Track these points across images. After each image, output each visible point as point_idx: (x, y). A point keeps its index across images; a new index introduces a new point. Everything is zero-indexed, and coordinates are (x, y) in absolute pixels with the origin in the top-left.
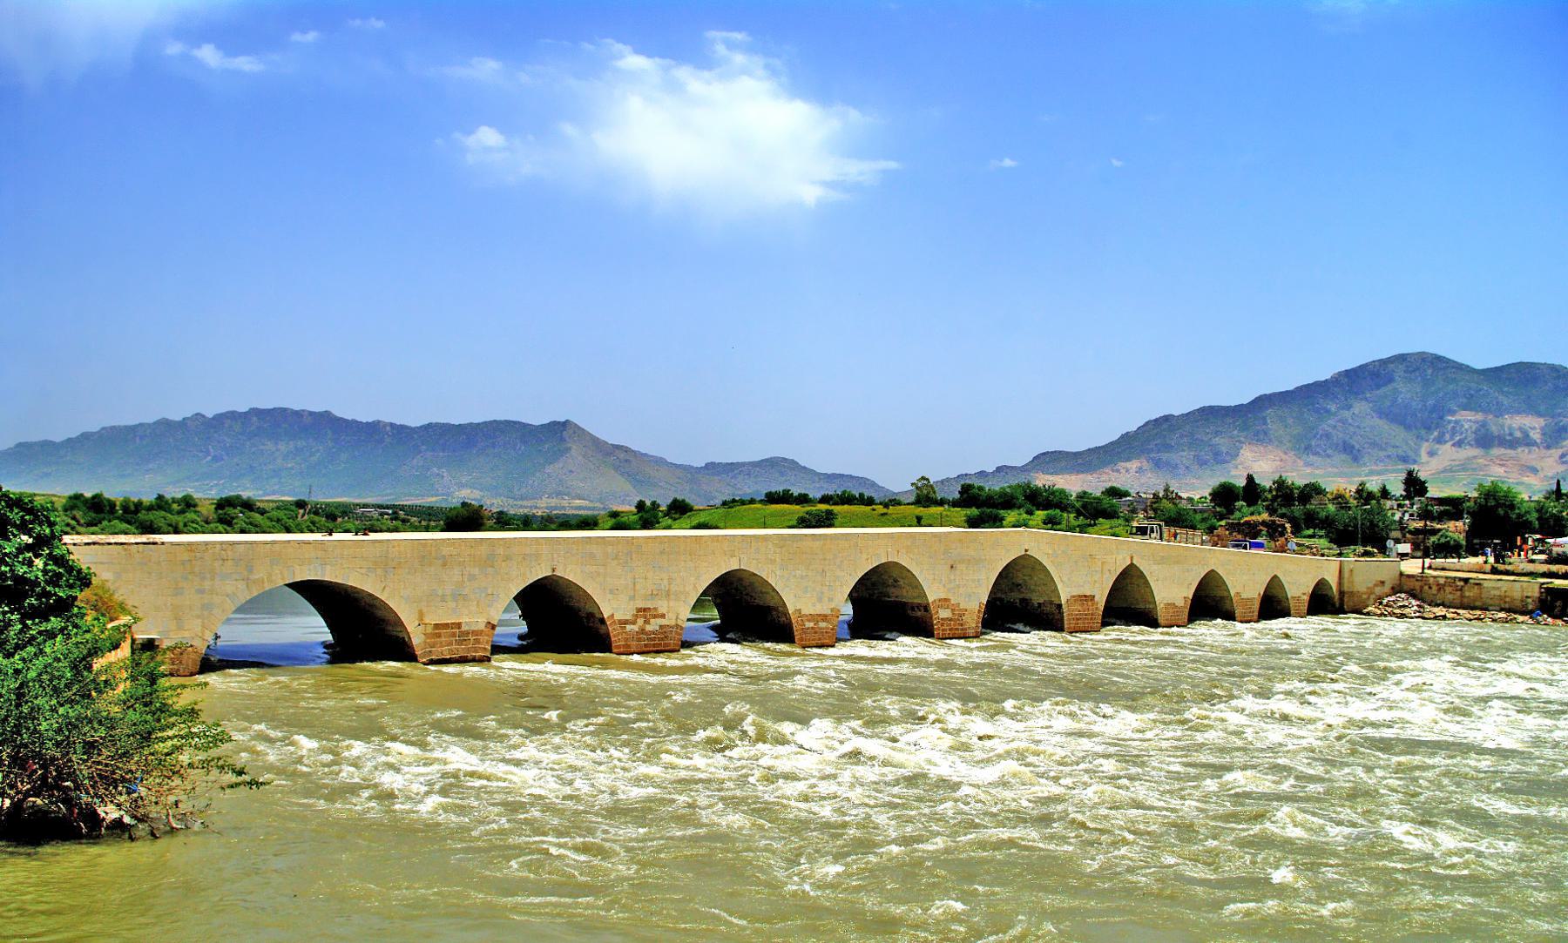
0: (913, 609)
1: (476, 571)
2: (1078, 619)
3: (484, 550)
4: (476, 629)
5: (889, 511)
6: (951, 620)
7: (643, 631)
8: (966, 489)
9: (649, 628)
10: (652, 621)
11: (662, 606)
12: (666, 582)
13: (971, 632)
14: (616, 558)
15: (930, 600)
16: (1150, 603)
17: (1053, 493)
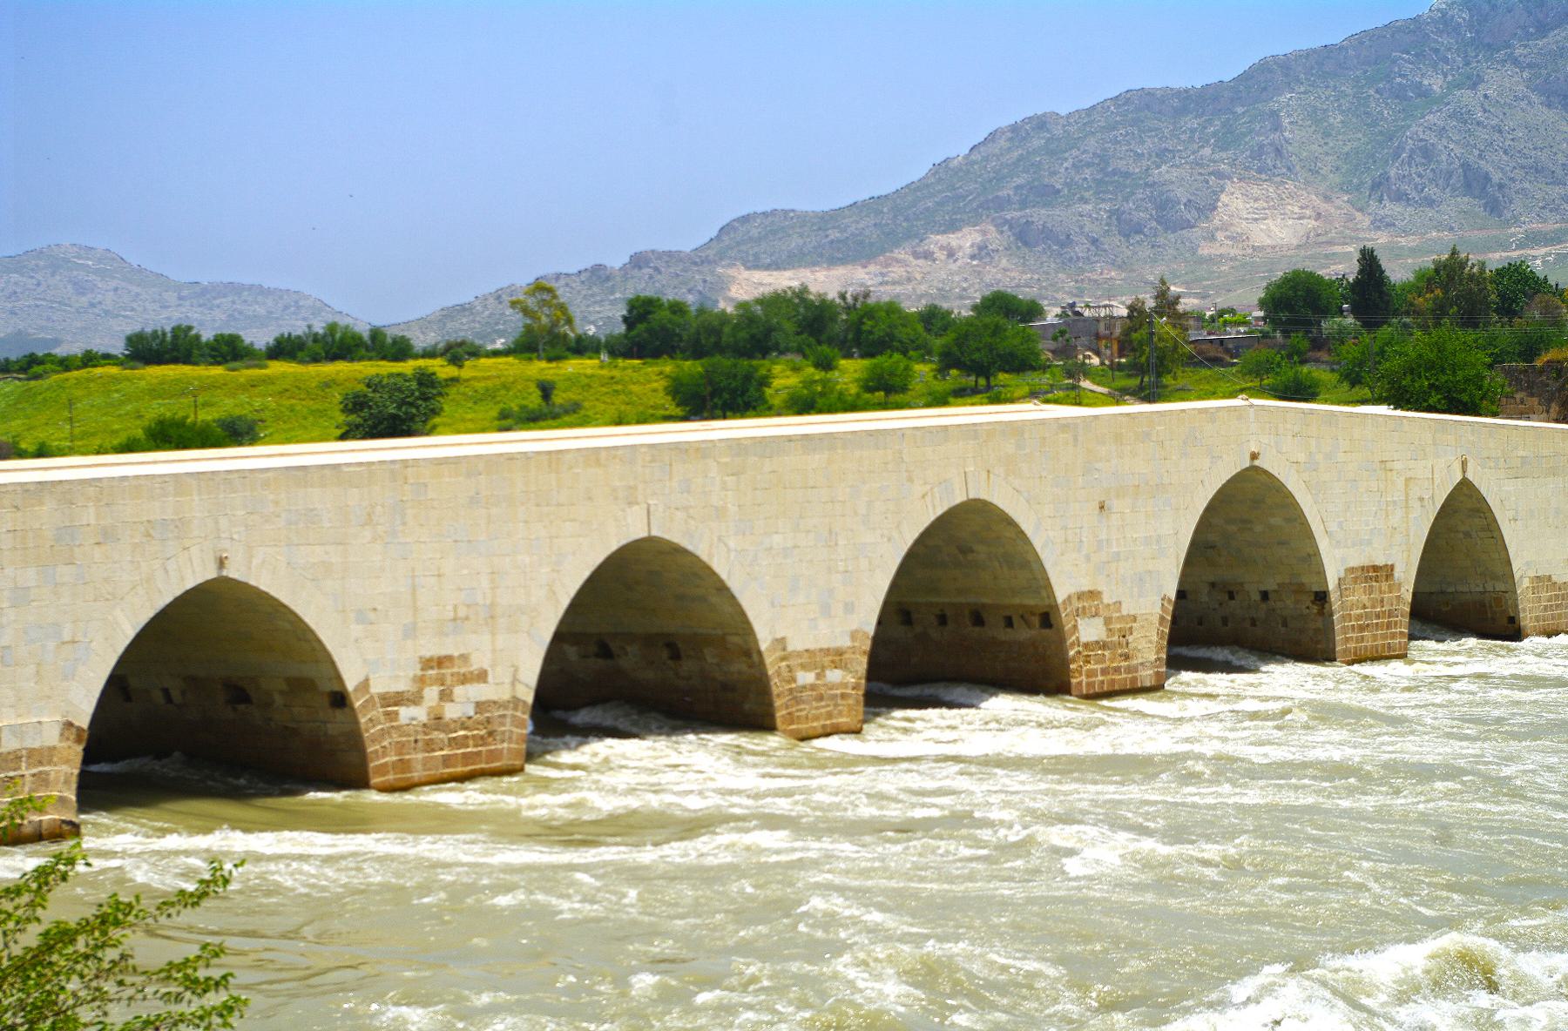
0: (1009, 622)
1: (30, 576)
2: (1362, 628)
3: (47, 513)
4: (37, 745)
5: (466, 373)
6: (1104, 646)
7: (437, 721)
8: (640, 311)
9: (452, 712)
10: (459, 691)
11: (479, 649)
12: (485, 583)
13: (1146, 676)
14: (369, 520)
15: (1060, 596)
16: (1495, 577)
17: (870, 313)
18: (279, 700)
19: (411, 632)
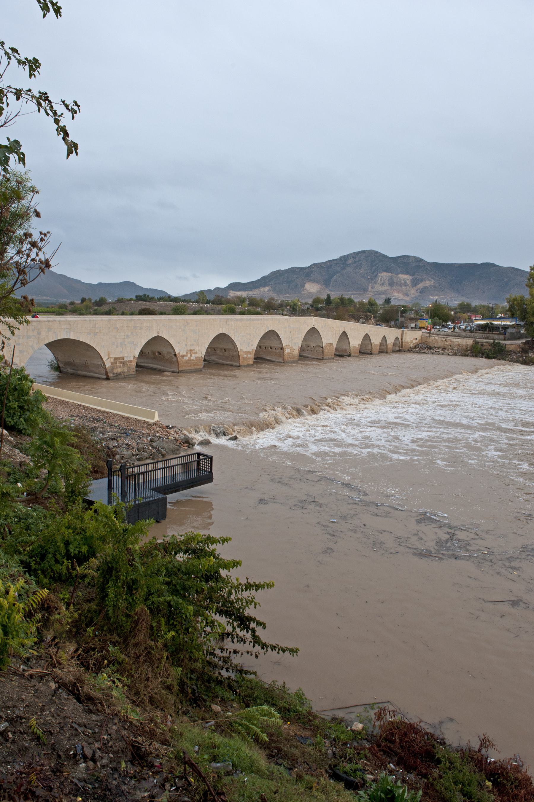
9: (192, 358)
10: (193, 355)
11: (197, 349)
15: (284, 345)
18: (166, 355)
19: (186, 345)
